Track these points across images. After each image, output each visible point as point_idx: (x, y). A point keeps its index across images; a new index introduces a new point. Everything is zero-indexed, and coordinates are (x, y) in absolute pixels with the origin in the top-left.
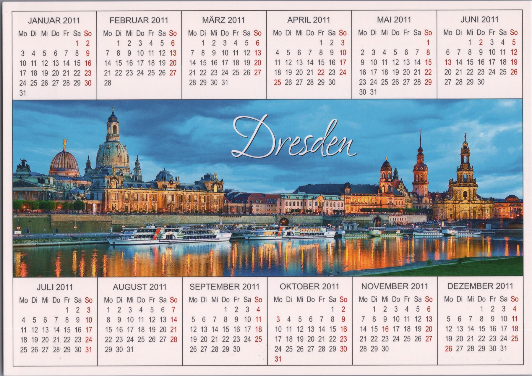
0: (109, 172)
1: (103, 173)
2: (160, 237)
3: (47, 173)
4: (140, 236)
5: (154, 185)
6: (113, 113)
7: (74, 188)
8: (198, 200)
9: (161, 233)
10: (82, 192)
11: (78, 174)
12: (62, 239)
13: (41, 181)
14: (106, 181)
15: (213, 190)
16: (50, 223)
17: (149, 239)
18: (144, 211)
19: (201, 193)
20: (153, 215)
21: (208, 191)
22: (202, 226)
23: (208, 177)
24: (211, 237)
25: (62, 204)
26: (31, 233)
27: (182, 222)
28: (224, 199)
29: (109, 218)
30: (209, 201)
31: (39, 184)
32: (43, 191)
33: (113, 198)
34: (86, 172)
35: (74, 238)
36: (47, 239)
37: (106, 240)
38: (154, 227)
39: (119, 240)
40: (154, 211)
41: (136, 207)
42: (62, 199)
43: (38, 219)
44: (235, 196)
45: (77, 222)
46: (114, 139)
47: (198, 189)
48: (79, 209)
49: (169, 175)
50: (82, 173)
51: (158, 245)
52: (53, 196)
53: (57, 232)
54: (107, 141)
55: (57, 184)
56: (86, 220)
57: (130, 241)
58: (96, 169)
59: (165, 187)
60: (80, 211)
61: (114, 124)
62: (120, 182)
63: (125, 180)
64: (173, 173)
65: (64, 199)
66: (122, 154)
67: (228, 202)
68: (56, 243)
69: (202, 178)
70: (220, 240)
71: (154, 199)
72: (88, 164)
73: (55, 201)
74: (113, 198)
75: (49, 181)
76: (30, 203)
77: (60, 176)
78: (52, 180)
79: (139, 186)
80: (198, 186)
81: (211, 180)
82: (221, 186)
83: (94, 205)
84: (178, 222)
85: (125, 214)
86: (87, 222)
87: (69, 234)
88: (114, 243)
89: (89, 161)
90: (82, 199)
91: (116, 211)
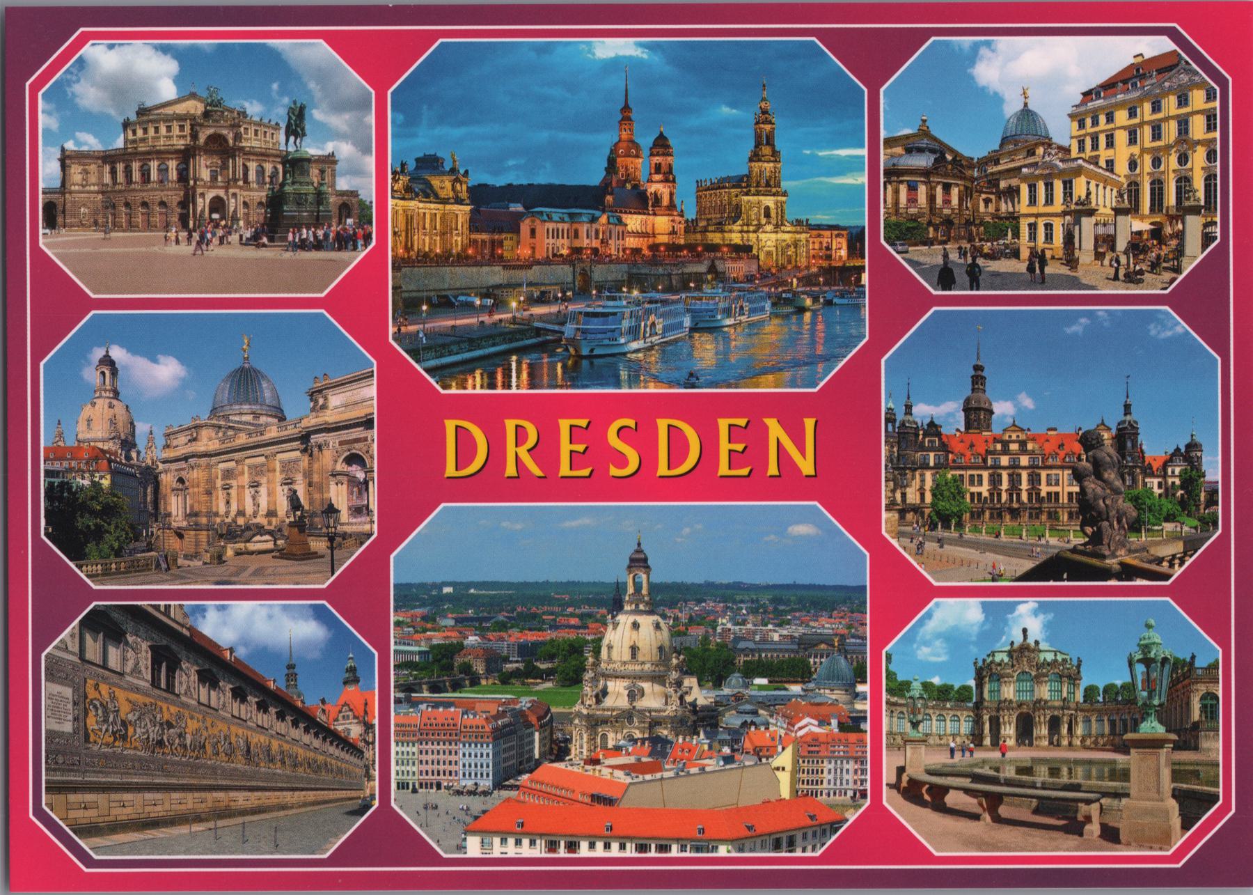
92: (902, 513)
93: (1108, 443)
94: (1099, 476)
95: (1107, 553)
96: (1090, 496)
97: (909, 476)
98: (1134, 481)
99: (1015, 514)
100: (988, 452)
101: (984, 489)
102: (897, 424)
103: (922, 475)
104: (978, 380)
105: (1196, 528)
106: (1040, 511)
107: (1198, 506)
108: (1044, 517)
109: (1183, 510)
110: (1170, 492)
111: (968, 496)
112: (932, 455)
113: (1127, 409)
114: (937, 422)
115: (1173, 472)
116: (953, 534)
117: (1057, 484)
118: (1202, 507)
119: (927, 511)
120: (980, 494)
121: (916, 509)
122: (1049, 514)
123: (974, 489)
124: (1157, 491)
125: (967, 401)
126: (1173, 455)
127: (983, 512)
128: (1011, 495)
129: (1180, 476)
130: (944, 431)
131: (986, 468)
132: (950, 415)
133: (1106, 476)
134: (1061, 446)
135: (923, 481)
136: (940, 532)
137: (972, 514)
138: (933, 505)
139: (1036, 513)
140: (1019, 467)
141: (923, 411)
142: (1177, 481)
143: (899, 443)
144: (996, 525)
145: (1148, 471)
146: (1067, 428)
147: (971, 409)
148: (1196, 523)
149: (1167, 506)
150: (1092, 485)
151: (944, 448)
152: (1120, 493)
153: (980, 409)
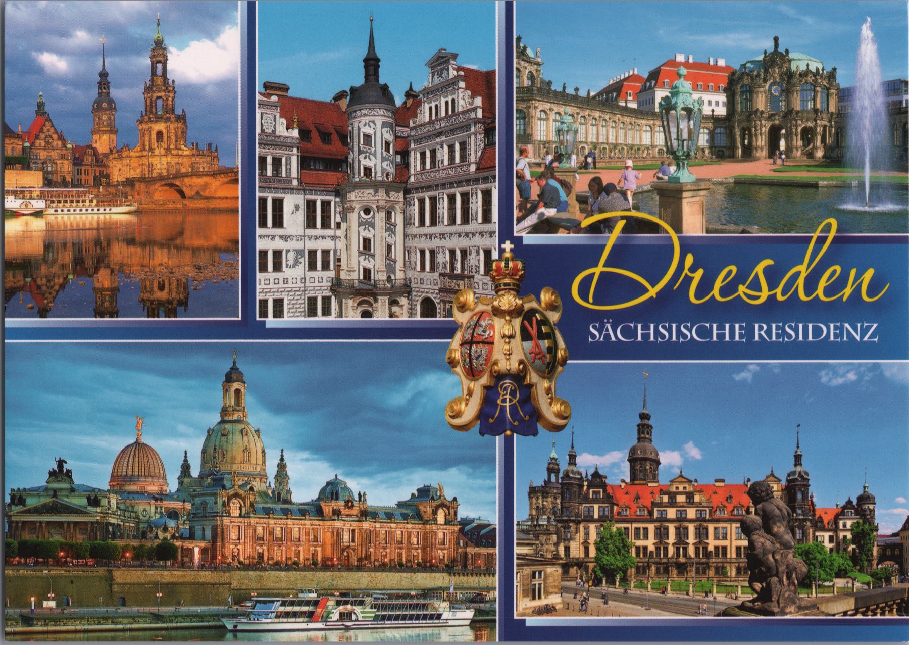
0: (227, 484)
1: (214, 486)
2: (327, 617)
3: (106, 487)
4: (287, 615)
5: (315, 510)
6: (234, 363)
7: (158, 516)
8: (405, 541)
9: (330, 607)
10: (171, 524)
11: (164, 488)
12: (133, 618)
13: (94, 501)
14: (220, 502)
15: (435, 520)
16: (111, 585)
17: (306, 620)
18: (295, 563)
19: (410, 526)
20: (313, 570)
21: (426, 523)
22: (413, 593)
23: (425, 492)
24: (432, 617)
25: (134, 548)
26: (73, 606)
27: (372, 585)
28: (458, 539)
29: (225, 577)
30: (427, 543)
31: (90, 509)
32: (97, 522)
33: (234, 536)
34: (181, 483)
35: (157, 617)
36: (105, 618)
37: (219, 620)
38: (315, 595)
39: (245, 620)
40: (315, 563)
41: (279, 554)
42: (134, 537)
43: (87, 577)
44: (483, 532)
45: (162, 584)
46: (235, 417)
47: (405, 517)
48: (166, 559)
49: (346, 488)
50: (173, 486)
51: (323, 633)
52: (117, 532)
53: (124, 605)
54: (223, 422)
55: (122, 507)
56: (181, 580)
57: (267, 623)
58: (201, 476)
59: (337, 513)
60: (169, 563)
61: (236, 386)
62: (248, 503)
63: (258, 499)
64: (354, 485)
65: (138, 538)
66: (252, 445)
67: (466, 545)
68: (120, 627)
69: (413, 495)
70: (451, 623)
71: (316, 539)
72: (186, 468)
73: (120, 543)
74: (234, 536)
75: (109, 502)
76: (71, 546)
77: (129, 493)
78: (114, 502)
79: (286, 513)
80: (404, 511)
81: (433, 498)
82: (452, 511)
83: (197, 550)
84: (363, 587)
85: (257, 569)
86: (183, 584)
87: (147, 609)
88: (235, 626)
89: (186, 460)
90: (173, 537)
91: (240, 563)
92: (566, 567)
93: (777, 495)
94: (768, 529)
95: (776, 610)
96: (759, 550)
97: (572, 529)
98: (805, 535)
99: (682, 568)
100: (654, 504)
101: (650, 543)
102: (561, 475)
103: (586, 528)
104: (644, 429)
105: (868, 584)
106: (707, 566)
107: (870, 561)
108: (711, 573)
109: (855, 565)
110: (842, 546)
111: (633, 551)
112: (596, 507)
113: (798, 459)
114: (601, 472)
115: (845, 526)
116: (618, 590)
117: (725, 538)
118: (875, 562)
119: (591, 565)
120: (645, 548)
121: (580, 564)
122: (717, 569)
123: (640, 543)
124: (828, 545)
125: (633, 451)
126: (844, 508)
127: (649, 567)
128: (678, 549)
129: (852, 530)
130: (608, 481)
131: (652, 521)
132: (615, 465)
133: (775, 529)
134: (729, 498)
135: (587, 534)
136: (604, 587)
137: (638, 568)
138: (597, 559)
139: (702, 569)
140: (686, 520)
141: (587, 462)
142: (849, 536)
143: (562, 494)
144: (662, 580)
145: (819, 525)
146: (736, 478)
147: (637, 459)
148: (868, 578)
149: (839, 561)
150: (762, 540)
151: (609, 499)
152: (790, 547)
153: (646, 459)
